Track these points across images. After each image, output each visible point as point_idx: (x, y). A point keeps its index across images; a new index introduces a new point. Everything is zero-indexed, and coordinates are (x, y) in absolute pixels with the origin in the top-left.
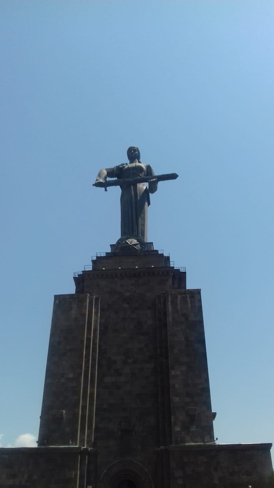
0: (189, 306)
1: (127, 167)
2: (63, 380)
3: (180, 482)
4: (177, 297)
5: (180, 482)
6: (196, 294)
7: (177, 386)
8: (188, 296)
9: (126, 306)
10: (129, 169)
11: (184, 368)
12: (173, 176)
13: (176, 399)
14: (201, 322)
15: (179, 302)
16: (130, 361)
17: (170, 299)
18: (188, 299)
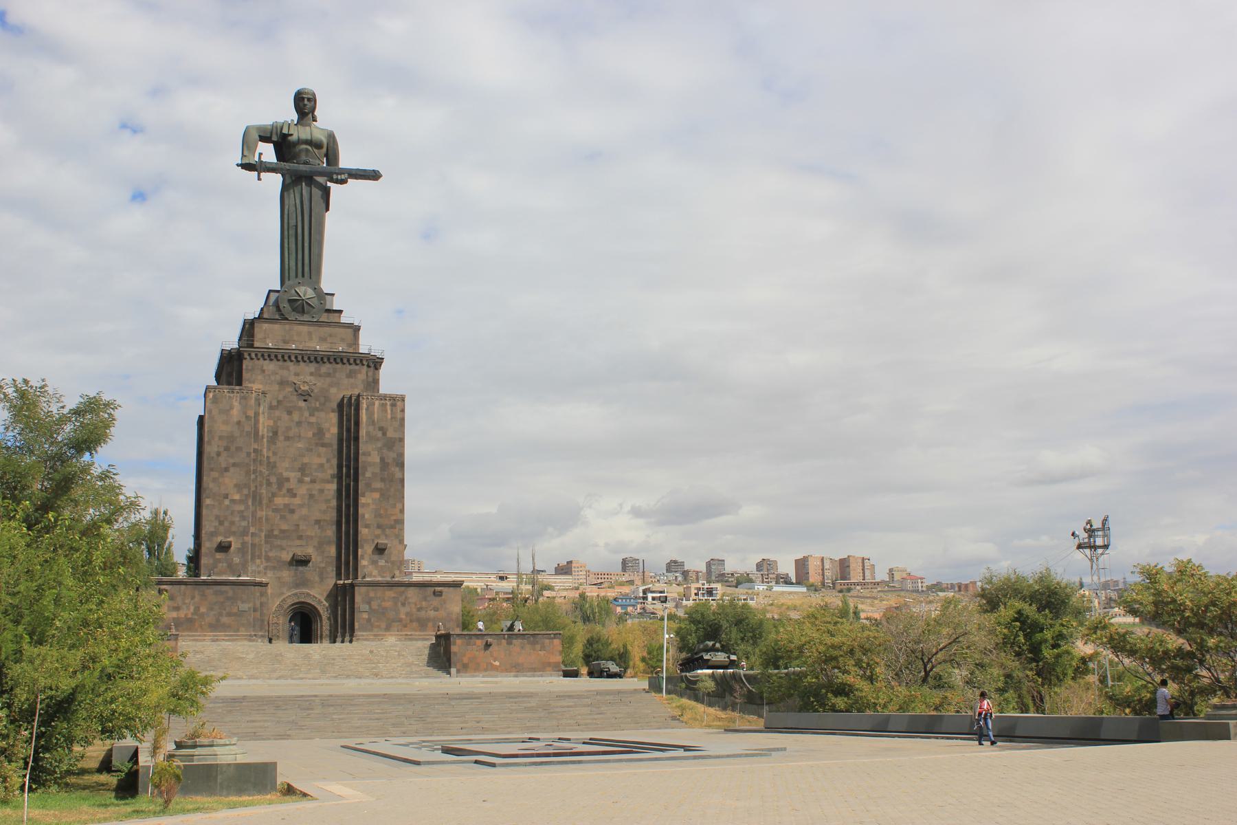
1: (294, 138)
2: (227, 502)
3: (365, 616)
5: (365, 616)
6: (397, 402)
7: (367, 516)
10: (300, 142)
11: (377, 495)
12: (374, 176)
13: (363, 532)
14: (402, 440)
16: (307, 479)
17: (365, 406)
18: (389, 407)
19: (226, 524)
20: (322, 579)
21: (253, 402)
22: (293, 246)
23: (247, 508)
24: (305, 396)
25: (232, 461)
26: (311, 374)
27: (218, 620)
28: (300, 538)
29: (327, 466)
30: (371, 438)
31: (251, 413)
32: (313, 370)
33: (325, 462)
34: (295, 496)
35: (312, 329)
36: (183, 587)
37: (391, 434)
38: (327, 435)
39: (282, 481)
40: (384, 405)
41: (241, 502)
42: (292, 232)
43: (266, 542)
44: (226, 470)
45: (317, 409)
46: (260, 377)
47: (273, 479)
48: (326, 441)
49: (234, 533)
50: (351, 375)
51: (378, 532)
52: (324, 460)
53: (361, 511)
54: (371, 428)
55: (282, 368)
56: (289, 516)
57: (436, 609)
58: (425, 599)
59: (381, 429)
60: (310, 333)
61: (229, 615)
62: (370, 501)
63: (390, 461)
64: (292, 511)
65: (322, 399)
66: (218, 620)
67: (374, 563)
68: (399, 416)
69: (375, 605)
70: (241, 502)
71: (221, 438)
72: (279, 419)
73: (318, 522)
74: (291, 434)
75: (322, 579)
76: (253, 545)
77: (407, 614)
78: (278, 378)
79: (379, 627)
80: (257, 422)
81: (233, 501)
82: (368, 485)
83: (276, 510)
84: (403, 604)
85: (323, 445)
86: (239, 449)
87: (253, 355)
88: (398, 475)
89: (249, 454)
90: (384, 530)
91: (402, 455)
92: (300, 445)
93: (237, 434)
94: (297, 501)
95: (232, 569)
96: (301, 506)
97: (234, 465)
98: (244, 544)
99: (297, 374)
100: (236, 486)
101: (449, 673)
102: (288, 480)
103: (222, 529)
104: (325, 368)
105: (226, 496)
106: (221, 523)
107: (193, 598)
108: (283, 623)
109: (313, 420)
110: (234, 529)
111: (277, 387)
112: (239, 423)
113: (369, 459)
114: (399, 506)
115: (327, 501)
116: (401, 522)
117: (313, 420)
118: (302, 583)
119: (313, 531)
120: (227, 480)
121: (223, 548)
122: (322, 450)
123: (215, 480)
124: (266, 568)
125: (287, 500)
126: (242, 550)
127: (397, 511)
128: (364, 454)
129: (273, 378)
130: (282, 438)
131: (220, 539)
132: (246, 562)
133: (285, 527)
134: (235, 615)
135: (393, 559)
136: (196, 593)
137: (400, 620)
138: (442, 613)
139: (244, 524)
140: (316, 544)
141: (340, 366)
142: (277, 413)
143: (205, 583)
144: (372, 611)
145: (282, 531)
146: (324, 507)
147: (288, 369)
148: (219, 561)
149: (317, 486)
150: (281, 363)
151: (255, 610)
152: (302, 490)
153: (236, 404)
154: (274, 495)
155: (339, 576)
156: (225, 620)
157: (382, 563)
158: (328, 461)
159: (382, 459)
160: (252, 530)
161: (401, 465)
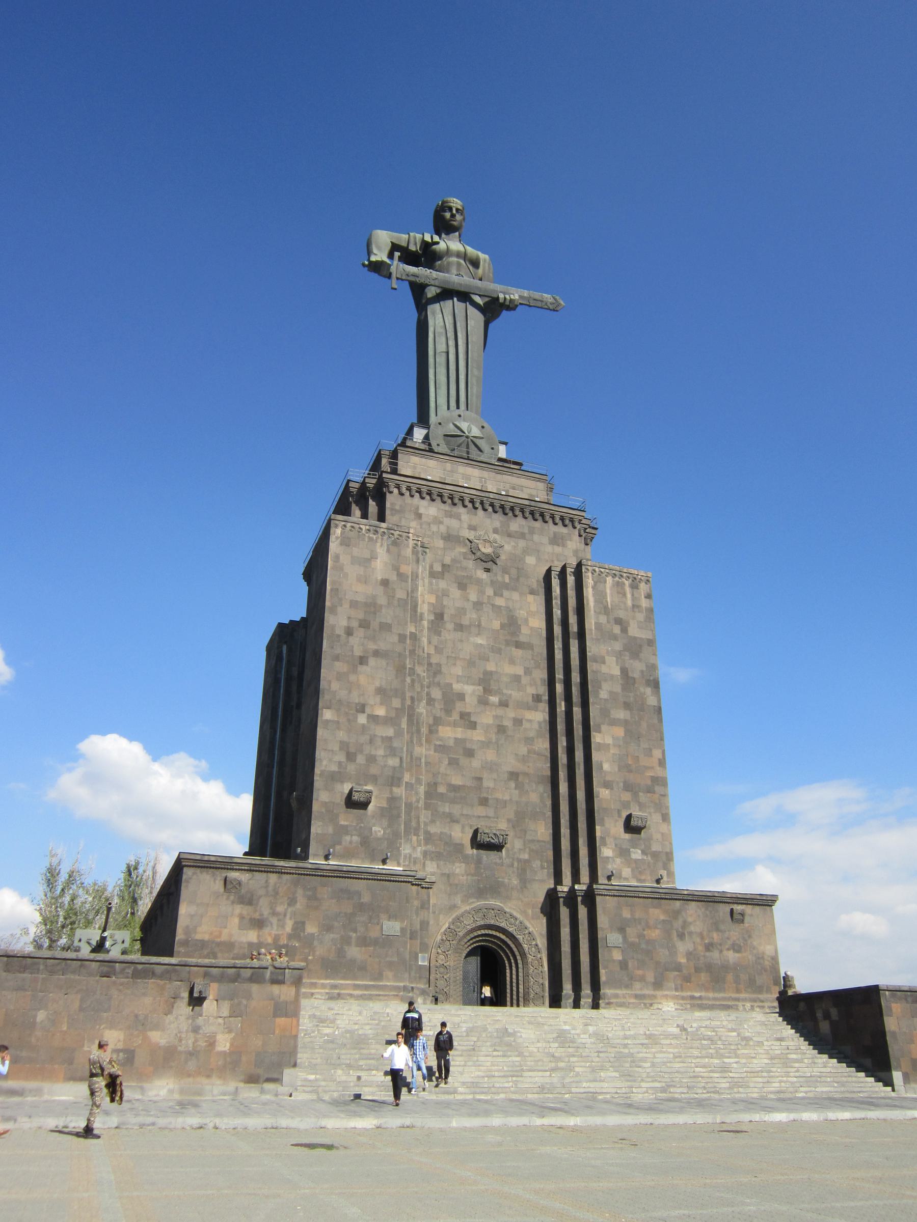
0: (629, 603)
2: (362, 719)
4: (605, 582)
5: (617, 956)
7: (606, 767)
8: (627, 583)
9: (483, 575)
10: (448, 252)
11: (620, 732)
13: (602, 794)
14: (651, 643)
15: (608, 591)
16: (494, 699)
19: (361, 759)
20: (524, 883)
21: (408, 552)
22: (444, 379)
23: (399, 733)
24: (489, 561)
25: (372, 646)
26: (495, 531)
27: (341, 953)
28: (484, 802)
29: (525, 680)
30: (606, 636)
31: (406, 569)
32: (497, 524)
33: (523, 675)
34: (473, 726)
35: (485, 474)
36: (273, 878)
37: (634, 631)
38: (525, 630)
39: (451, 699)
40: (619, 585)
41: (387, 721)
42: (441, 360)
43: (427, 806)
44: (363, 660)
45: (507, 587)
46: (413, 524)
47: (436, 694)
48: (522, 639)
49: (374, 779)
50: (556, 540)
51: (627, 796)
52: (519, 671)
53: (596, 756)
54: (603, 619)
55: (451, 516)
56: (464, 761)
57: (736, 948)
58: (716, 926)
59: (618, 621)
61: (364, 942)
62: (609, 740)
63: (636, 675)
64: (470, 753)
65: (514, 572)
66: (341, 953)
67: (623, 853)
68: (644, 603)
69: (632, 933)
70: (387, 721)
71: (354, 604)
72: (445, 593)
73: (514, 776)
74: (465, 621)
75: (524, 883)
76: (409, 806)
77: (689, 955)
78: (443, 529)
79: (642, 979)
80: (415, 589)
81: (373, 718)
82: (605, 713)
83: (442, 749)
84: (681, 936)
85: (518, 645)
86: (386, 627)
87: (404, 490)
88: (652, 701)
89: (402, 638)
90: (635, 795)
91: (653, 667)
92: (479, 641)
93: (382, 600)
94: (477, 736)
95: (367, 845)
96: (486, 744)
97: (376, 653)
98: (392, 800)
99: (472, 528)
100: (380, 691)
101: (889, 1083)
102: (461, 697)
103: (351, 768)
104: (517, 524)
105: (362, 709)
106: (351, 757)
107: (292, 902)
108: (459, 966)
109: (500, 602)
110: (374, 770)
111: (440, 544)
112: (385, 583)
113: (604, 669)
114: (657, 753)
115: (529, 740)
116: (662, 782)
117: (500, 602)
118: (488, 887)
119: (507, 793)
120: (363, 680)
121: (354, 803)
122: (518, 653)
123: (340, 677)
124: (425, 854)
125: (459, 733)
126: (390, 812)
127: (654, 761)
128: (595, 660)
129: (434, 528)
130: (450, 626)
131: (346, 788)
132: (397, 835)
133: (457, 780)
134: (375, 942)
135: (655, 847)
136: (300, 892)
137: (678, 968)
138: (748, 957)
139: (393, 762)
140: (512, 816)
141: (538, 524)
142: (442, 584)
143: (317, 872)
144: (629, 947)
145: (454, 788)
146: (523, 750)
147: (458, 517)
148: (345, 830)
149: (511, 713)
150: (446, 507)
151: (413, 936)
152: (486, 718)
153: (381, 550)
154: (437, 721)
155: (558, 879)
156: (354, 952)
157: (636, 854)
158: (527, 671)
159: (624, 671)
160: (407, 777)
161: (655, 685)
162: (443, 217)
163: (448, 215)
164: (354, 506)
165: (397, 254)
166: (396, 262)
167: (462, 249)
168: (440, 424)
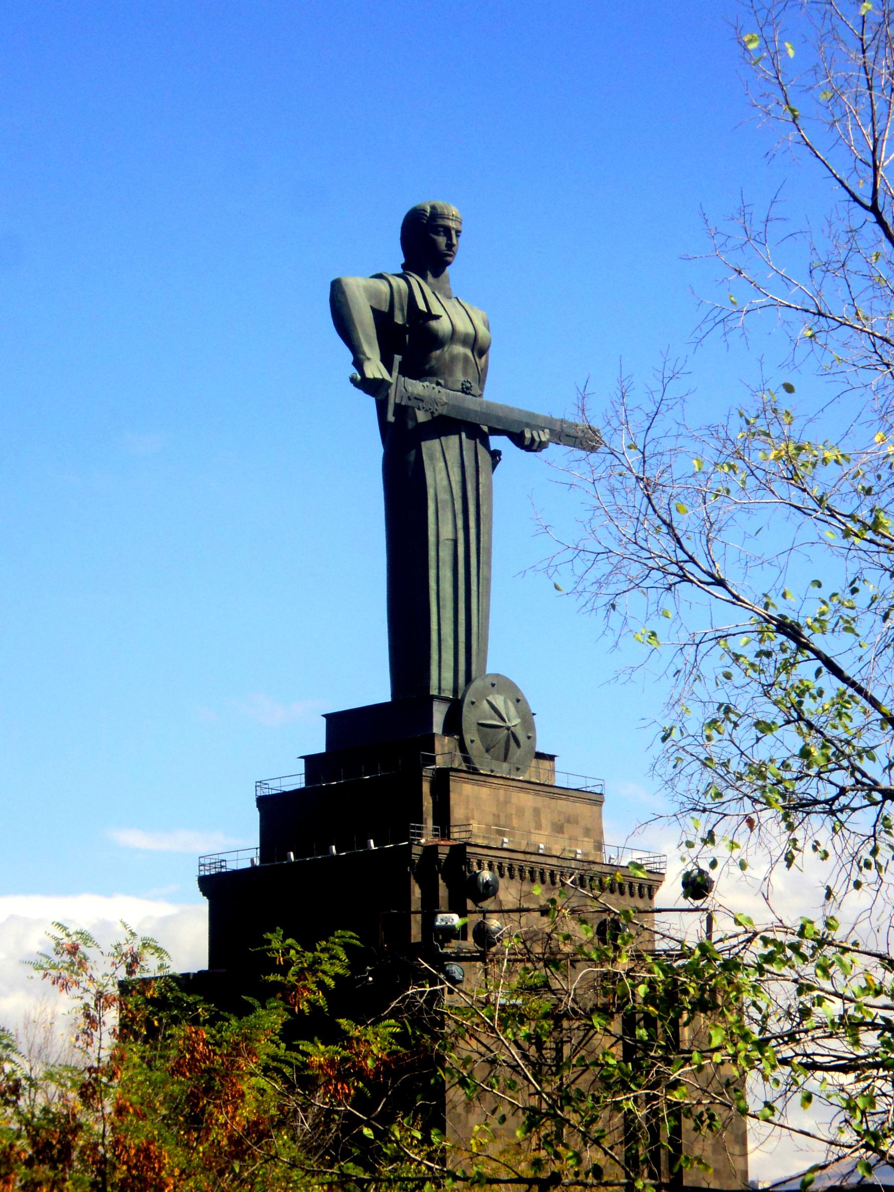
10: (454, 335)
42: (446, 554)
60: (537, 812)
162: (434, 243)
163: (442, 240)
164: (413, 882)
165: (398, 358)
166: (395, 374)
167: (471, 331)
168: (473, 703)
